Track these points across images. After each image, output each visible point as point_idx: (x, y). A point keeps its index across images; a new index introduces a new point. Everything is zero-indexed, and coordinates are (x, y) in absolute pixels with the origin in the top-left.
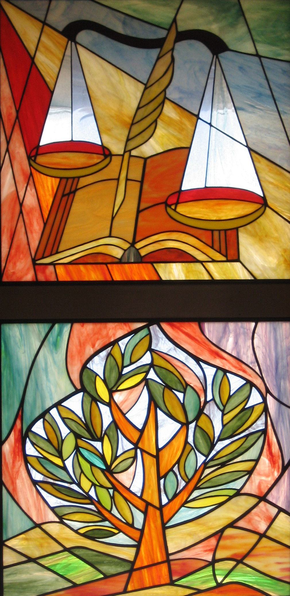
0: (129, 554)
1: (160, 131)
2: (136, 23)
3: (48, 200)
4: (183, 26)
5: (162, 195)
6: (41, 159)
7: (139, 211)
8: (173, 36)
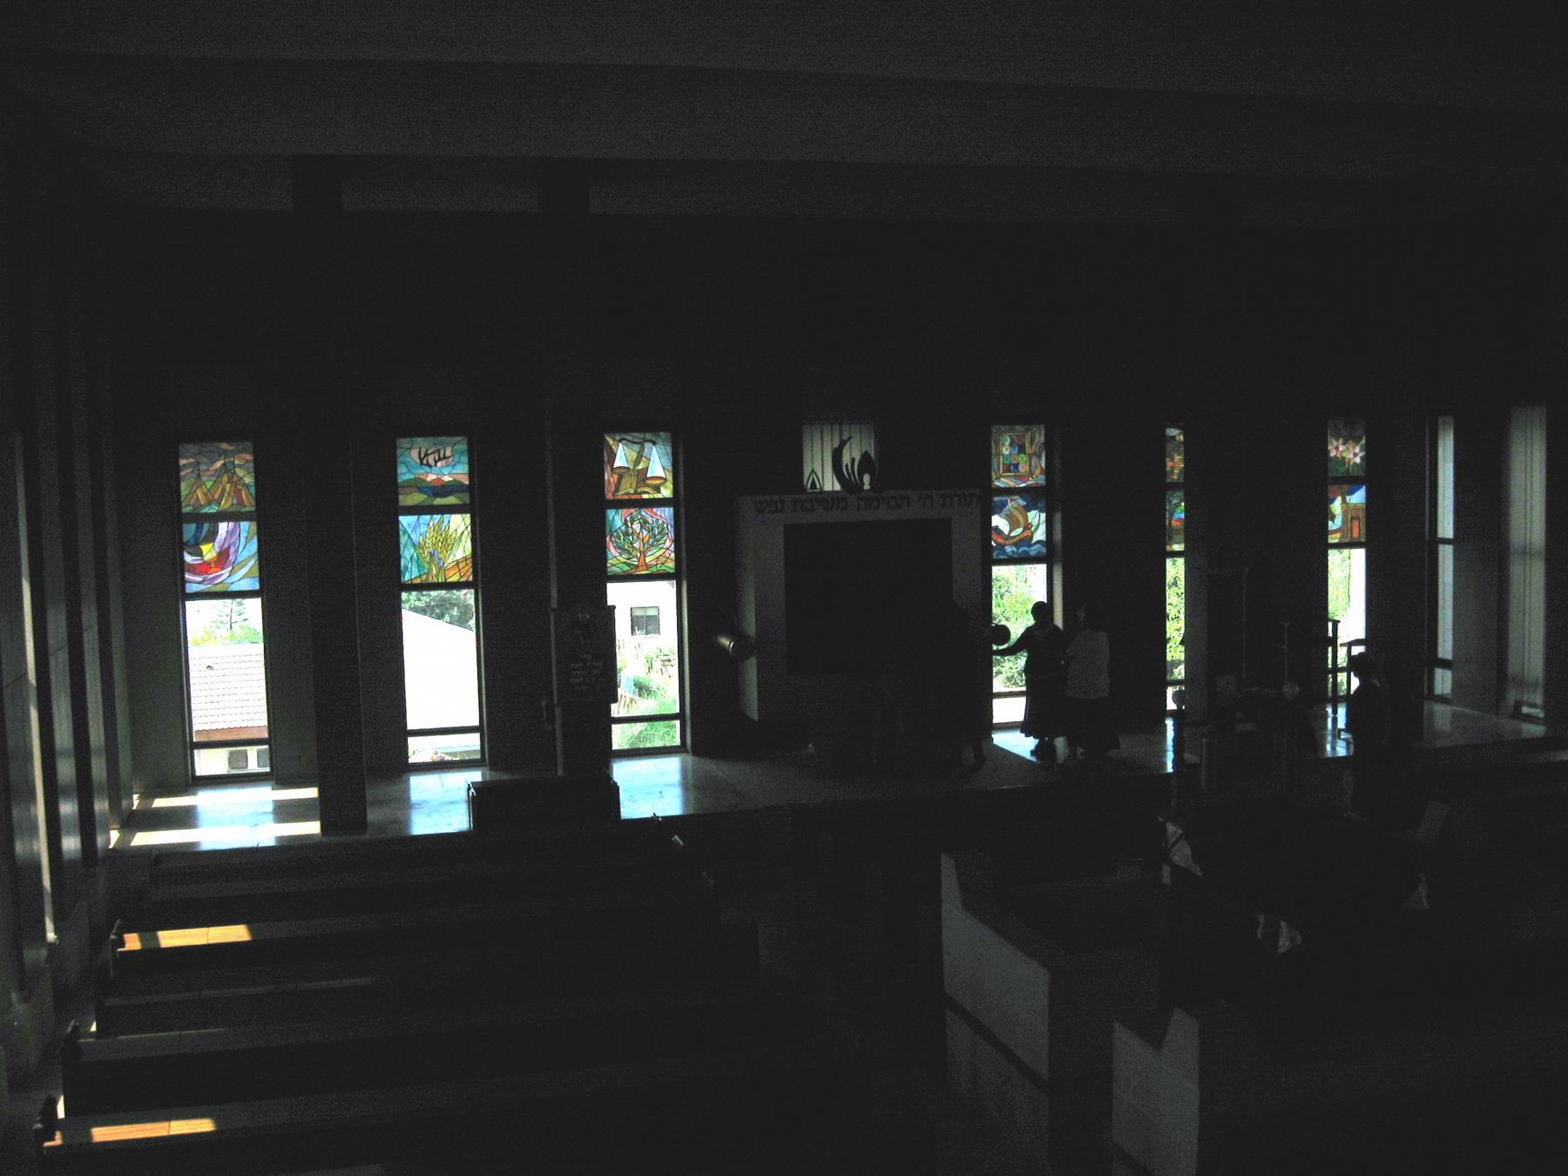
0: (636, 563)
1: (642, 463)
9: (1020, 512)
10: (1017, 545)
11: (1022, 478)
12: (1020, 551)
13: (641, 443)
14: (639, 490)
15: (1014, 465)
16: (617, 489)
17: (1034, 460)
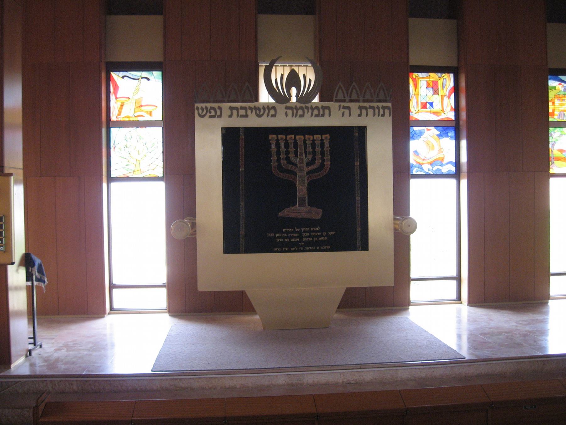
2: (135, 76)
3: (119, 107)
4: (142, 76)
5: (139, 105)
6: (118, 99)
7: (135, 108)
8: (141, 78)
9: (435, 140)
10: (431, 164)
11: (435, 113)
12: (434, 169)
13: (138, 79)
14: (136, 115)
15: (429, 103)
16: (119, 114)
17: (446, 99)
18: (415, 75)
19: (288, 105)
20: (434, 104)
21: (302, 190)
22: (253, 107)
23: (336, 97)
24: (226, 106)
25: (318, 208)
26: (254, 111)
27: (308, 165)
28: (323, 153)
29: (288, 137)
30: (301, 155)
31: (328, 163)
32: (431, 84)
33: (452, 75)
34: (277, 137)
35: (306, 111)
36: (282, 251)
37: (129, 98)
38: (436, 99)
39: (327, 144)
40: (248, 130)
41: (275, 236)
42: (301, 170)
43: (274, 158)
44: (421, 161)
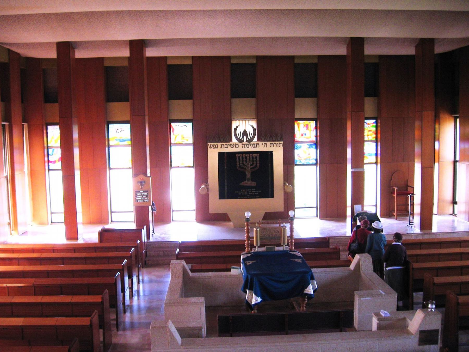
15: (304, 134)
16: (175, 141)
18: (298, 122)
19: (243, 143)
20: (306, 134)
21: (248, 175)
22: (230, 144)
23: (261, 140)
24: (219, 144)
25: (255, 182)
26: (230, 146)
27: (251, 165)
28: (256, 161)
29: (243, 155)
30: (248, 162)
31: (258, 165)
32: (305, 126)
33: (315, 122)
34: (239, 155)
35: (250, 145)
36: (241, 198)
37: (179, 134)
38: (307, 132)
39: (258, 159)
40: (228, 153)
41: (238, 192)
42: (248, 168)
43: (238, 163)
44: (301, 159)
